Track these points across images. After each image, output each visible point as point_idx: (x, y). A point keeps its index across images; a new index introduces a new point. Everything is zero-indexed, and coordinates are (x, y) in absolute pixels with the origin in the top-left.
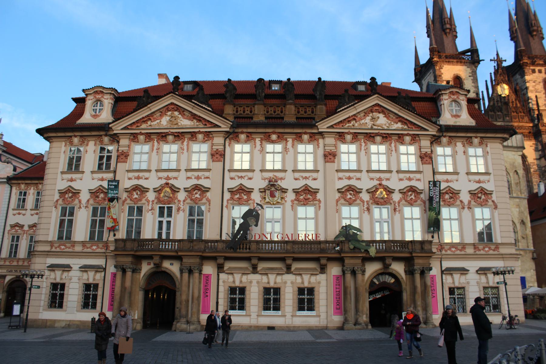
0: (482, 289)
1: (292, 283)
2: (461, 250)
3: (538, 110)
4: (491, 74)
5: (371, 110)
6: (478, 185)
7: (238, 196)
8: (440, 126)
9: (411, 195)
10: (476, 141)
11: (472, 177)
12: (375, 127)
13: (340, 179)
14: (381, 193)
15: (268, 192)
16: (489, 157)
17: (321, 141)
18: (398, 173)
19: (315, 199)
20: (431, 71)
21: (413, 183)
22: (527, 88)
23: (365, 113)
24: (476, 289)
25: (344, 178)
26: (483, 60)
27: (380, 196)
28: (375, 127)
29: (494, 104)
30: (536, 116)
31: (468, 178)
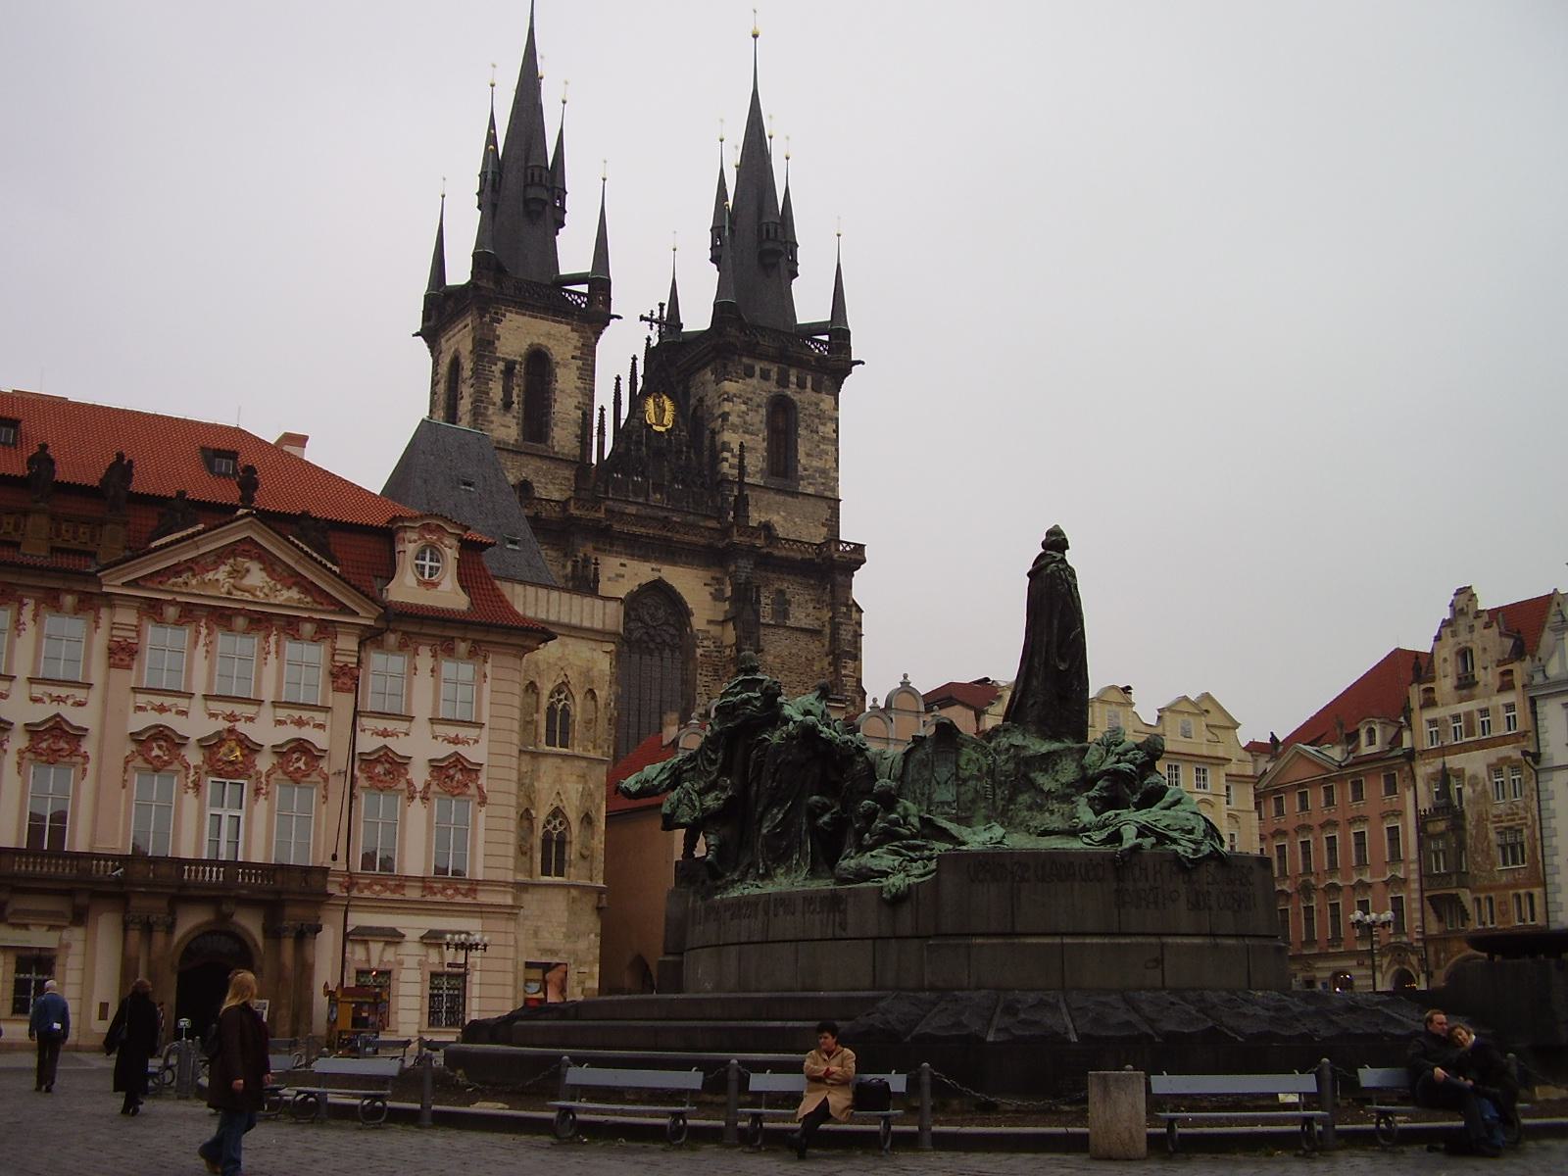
0: (428, 977)
2: (393, 892)
3: (741, 484)
4: (634, 359)
6: (451, 749)
8: (387, 607)
9: (298, 760)
10: (462, 647)
11: (441, 729)
12: (235, 592)
13: (140, 708)
14: (232, 751)
16: (487, 687)
17: (104, 613)
18: (275, 707)
19: (74, 752)
20: (469, 320)
21: (307, 733)
22: (725, 416)
23: (219, 557)
24: (416, 976)
25: (149, 708)
26: (619, 317)
27: (229, 758)
28: (237, 595)
29: (628, 449)
30: (731, 499)
31: (433, 731)
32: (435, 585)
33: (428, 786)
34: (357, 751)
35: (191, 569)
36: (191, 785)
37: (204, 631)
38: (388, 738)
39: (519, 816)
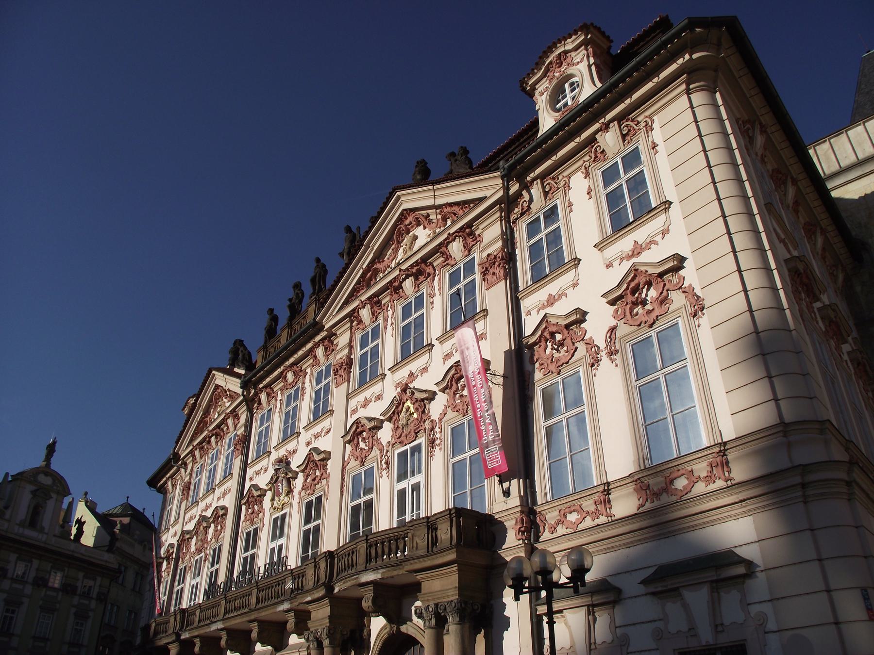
2: (596, 514)
33: (613, 329)
35: (376, 272)
36: (384, 466)
38: (556, 304)
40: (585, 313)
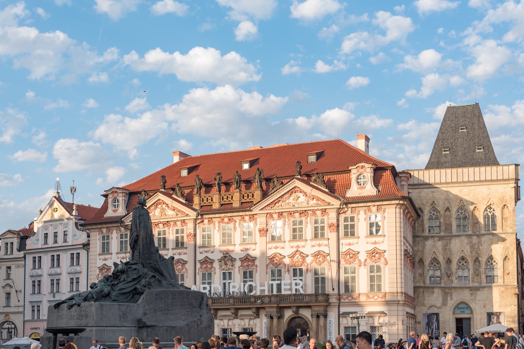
1: (239, 325)
5: (291, 192)
6: (374, 246)
7: (204, 266)
9: (320, 258)
10: (374, 209)
15: (223, 261)
16: (386, 222)
17: (258, 220)
32: (364, 188)
34: (341, 251)
37: (287, 220)
39: (473, 261)
40: (359, 252)
